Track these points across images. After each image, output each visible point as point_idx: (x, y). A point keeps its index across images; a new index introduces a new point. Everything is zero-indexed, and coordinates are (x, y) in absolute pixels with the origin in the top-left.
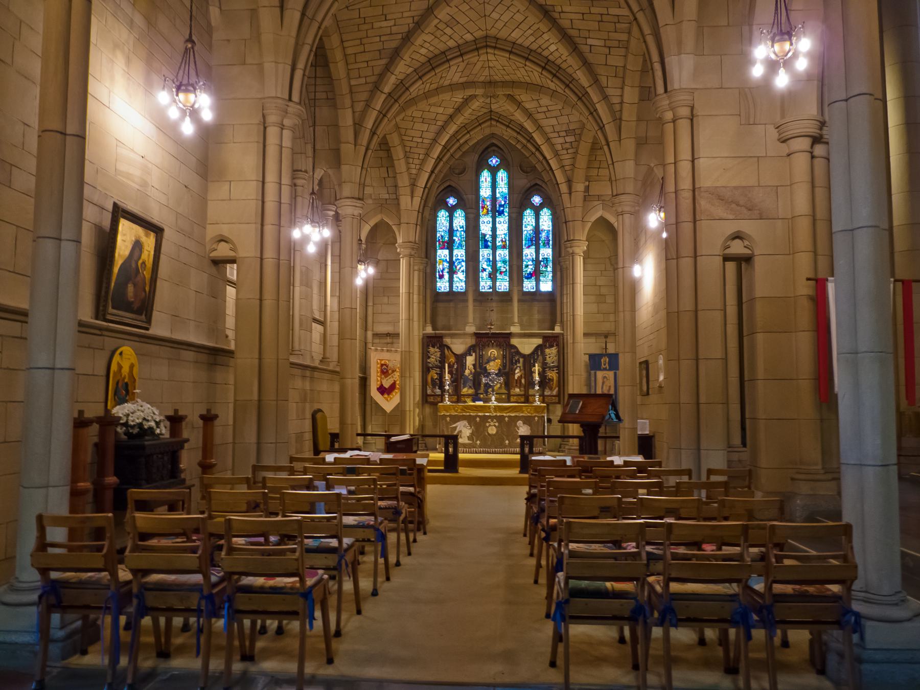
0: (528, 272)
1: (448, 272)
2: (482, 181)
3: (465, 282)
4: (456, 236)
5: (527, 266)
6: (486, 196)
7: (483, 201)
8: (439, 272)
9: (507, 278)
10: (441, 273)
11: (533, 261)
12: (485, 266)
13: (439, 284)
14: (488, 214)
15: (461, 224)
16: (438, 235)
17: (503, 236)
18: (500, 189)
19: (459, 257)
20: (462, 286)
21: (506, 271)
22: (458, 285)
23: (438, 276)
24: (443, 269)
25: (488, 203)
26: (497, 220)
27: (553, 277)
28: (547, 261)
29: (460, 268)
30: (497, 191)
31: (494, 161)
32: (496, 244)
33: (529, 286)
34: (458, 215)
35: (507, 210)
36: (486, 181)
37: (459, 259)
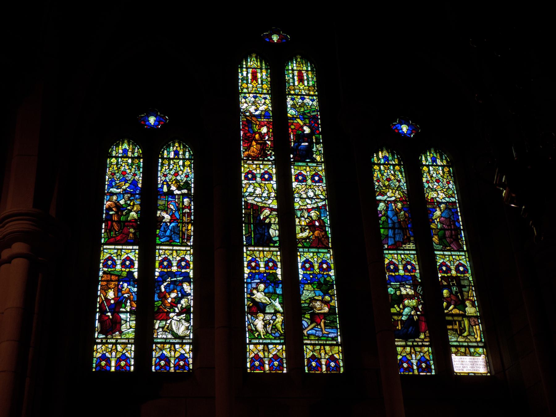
0: (404, 318)
1: (131, 312)
2: (245, 79)
3: (196, 344)
4: (166, 209)
5: (400, 299)
6: (257, 113)
7: (249, 123)
8: (103, 312)
9: (336, 334)
10: (109, 314)
11: (414, 286)
12: (259, 296)
13: (99, 350)
14: (266, 155)
15: (181, 177)
16: (107, 204)
17: (313, 214)
18: (298, 100)
19: (174, 269)
20: (182, 357)
21: (332, 309)
22: (166, 353)
23: (97, 324)
24: (119, 302)
25: (264, 130)
26: (294, 171)
27: (486, 332)
28: (461, 287)
29: (177, 300)
30: (290, 102)
31: (275, 38)
32: (295, 234)
33: (414, 362)
34: (172, 155)
35: (320, 147)
36: (255, 78)
37: (174, 275)
